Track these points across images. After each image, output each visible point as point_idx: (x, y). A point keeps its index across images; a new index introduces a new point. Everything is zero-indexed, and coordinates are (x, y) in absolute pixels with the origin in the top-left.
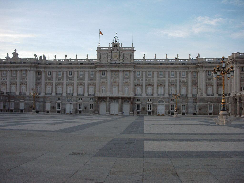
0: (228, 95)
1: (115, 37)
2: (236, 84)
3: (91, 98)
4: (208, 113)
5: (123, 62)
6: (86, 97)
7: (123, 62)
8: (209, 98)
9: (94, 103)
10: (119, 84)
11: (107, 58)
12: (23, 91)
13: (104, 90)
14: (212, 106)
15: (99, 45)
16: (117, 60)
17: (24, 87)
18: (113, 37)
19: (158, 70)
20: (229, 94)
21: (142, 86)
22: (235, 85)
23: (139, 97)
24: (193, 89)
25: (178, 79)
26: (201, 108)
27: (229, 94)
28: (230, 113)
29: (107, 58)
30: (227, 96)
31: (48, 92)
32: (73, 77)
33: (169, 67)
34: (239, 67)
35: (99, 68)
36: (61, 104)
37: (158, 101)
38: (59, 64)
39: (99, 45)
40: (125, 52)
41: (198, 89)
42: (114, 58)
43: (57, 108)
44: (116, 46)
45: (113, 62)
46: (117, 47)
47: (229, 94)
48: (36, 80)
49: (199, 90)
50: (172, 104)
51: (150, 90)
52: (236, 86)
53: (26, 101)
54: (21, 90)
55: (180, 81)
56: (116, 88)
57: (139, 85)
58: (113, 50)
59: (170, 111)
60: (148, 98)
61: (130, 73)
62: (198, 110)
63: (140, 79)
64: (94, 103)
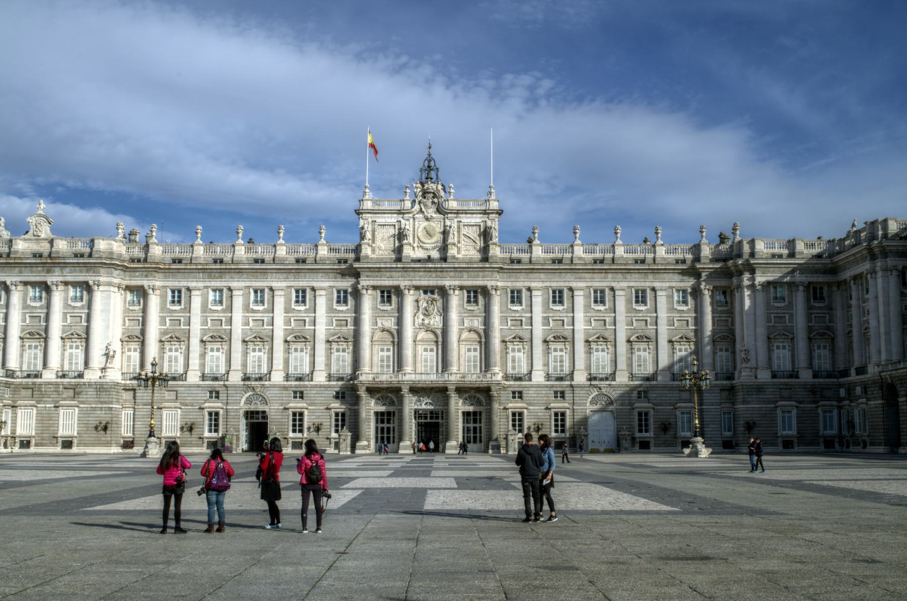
0: (853, 372)
1: (426, 164)
2: (888, 333)
4: (780, 440)
5: (459, 252)
6: (321, 386)
7: (459, 252)
8: (781, 387)
9: (350, 409)
12: (71, 364)
13: (519, 359)
14: (794, 412)
17: (74, 351)
18: (420, 163)
19: (589, 284)
20: (857, 369)
22: (883, 337)
23: (520, 386)
24: (719, 354)
25: (663, 314)
26: (754, 423)
27: (861, 370)
28: (866, 438)
30: (850, 379)
31: (170, 366)
32: (269, 312)
33: (629, 271)
34: (897, 270)
35: (367, 276)
36: (221, 412)
37: (589, 400)
38: (215, 261)
40: (465, 219)
41: (737, 352)
42: (422, 239)
43: (206, 428)
44: (432, 195)
45: (420, 254)
46: (433, 197)
47: (857, 369)
48: (124, 321)
49: (740, 356)
50: (643, 410)
51: (561, 356)
52: (888, 341)
53: (83, 403)
54: (63, 360)
55: (671, 323)
59: (638, 435)
60: (552, 386)
62: (742, 429)
63: (524, 319)
64: (350, 409)
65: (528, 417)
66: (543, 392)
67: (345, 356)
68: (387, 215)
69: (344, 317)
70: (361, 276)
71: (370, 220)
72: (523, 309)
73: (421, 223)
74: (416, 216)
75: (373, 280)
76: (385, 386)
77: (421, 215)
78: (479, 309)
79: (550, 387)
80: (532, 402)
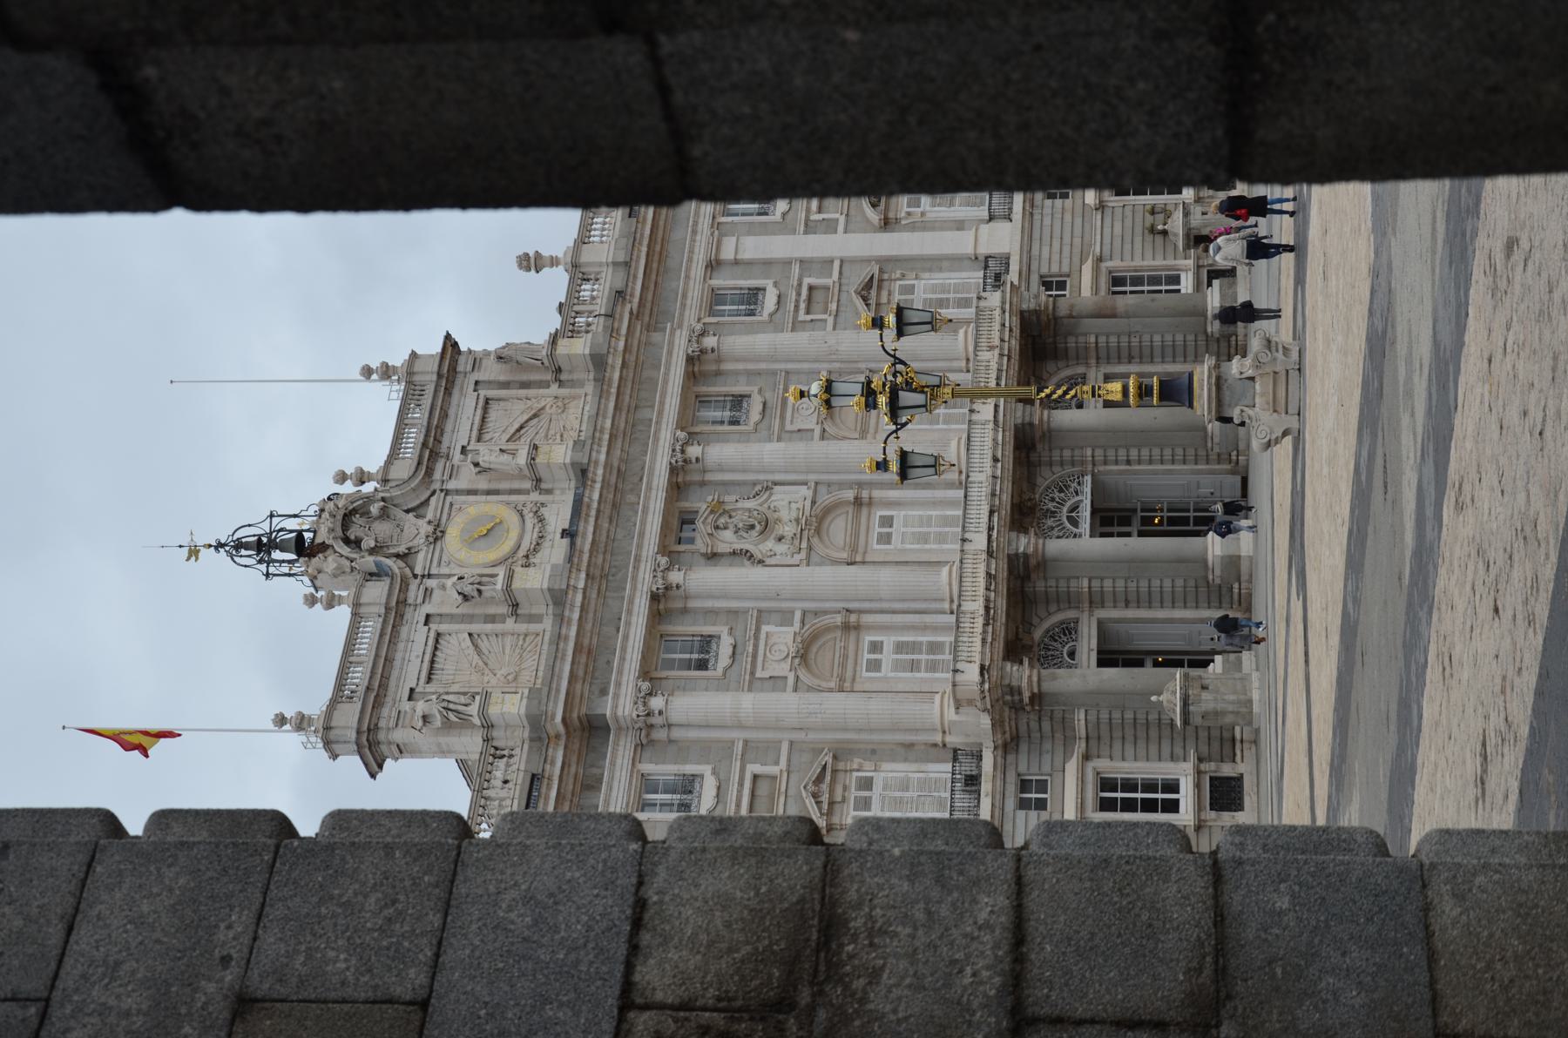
3: (1010, 803)
9: (1087, 757)
10: (842, 485)
11: (489, 627)
15: (301, 723)
16: (541, 520)
21: (885, 262)
29: (491, 619)
35: (604, 692)
39: (301, 723)
44: (357, 519)
45: (556, 551)
56: (887, 521)
57: (868, 285)
58: (406, 557)
61: (718, 373)
63: (807, 281)
64: (1087, 757)
65: (1127, 255)
66: (1047, 221)
67: (885, 779)
68: (399, 656)
69: (741, 784)
70: (599, 711)
71: (406, 706)
72: (776, 284)
73: (445, 558)
74: (418, 570)
75: (620, 672)
76: (1001, 604)
77: (421, 556)
78: (760, 391)
79: (1032, 206)
80: (1077, 250)
